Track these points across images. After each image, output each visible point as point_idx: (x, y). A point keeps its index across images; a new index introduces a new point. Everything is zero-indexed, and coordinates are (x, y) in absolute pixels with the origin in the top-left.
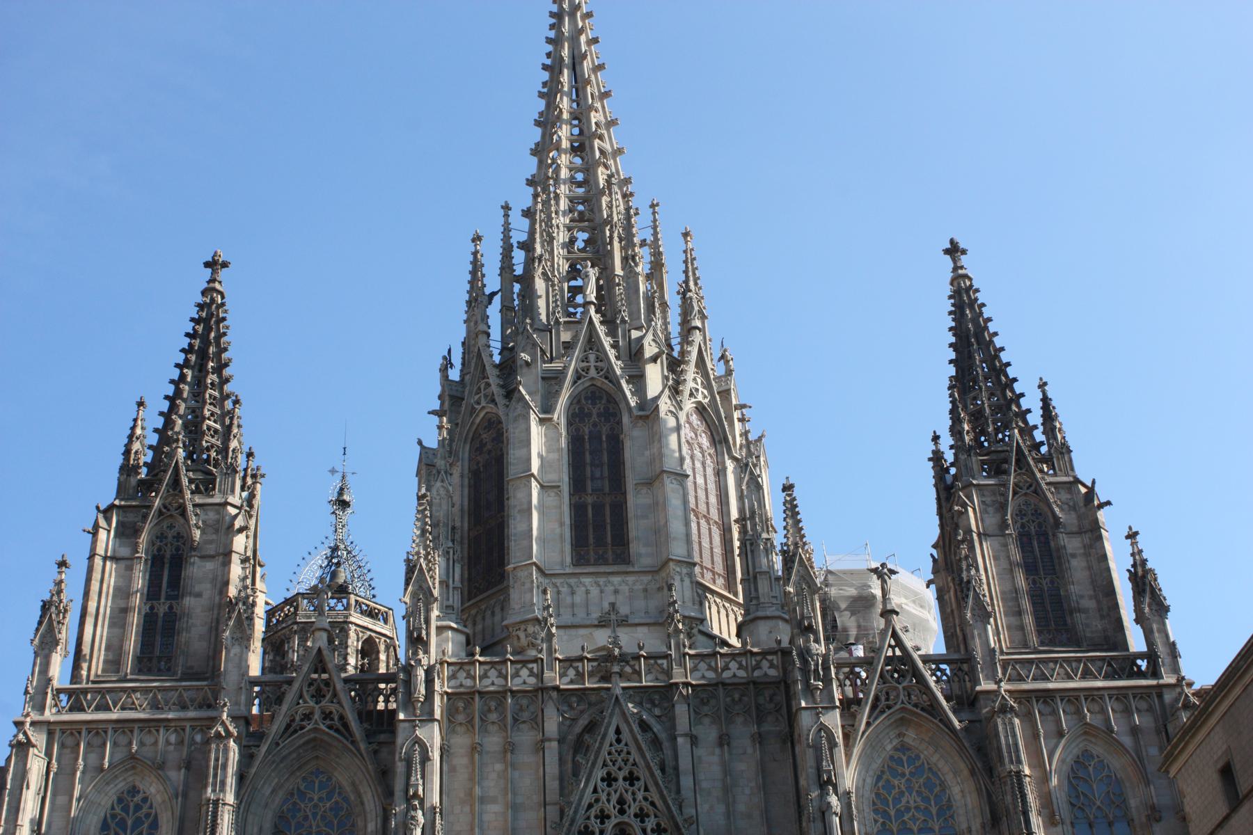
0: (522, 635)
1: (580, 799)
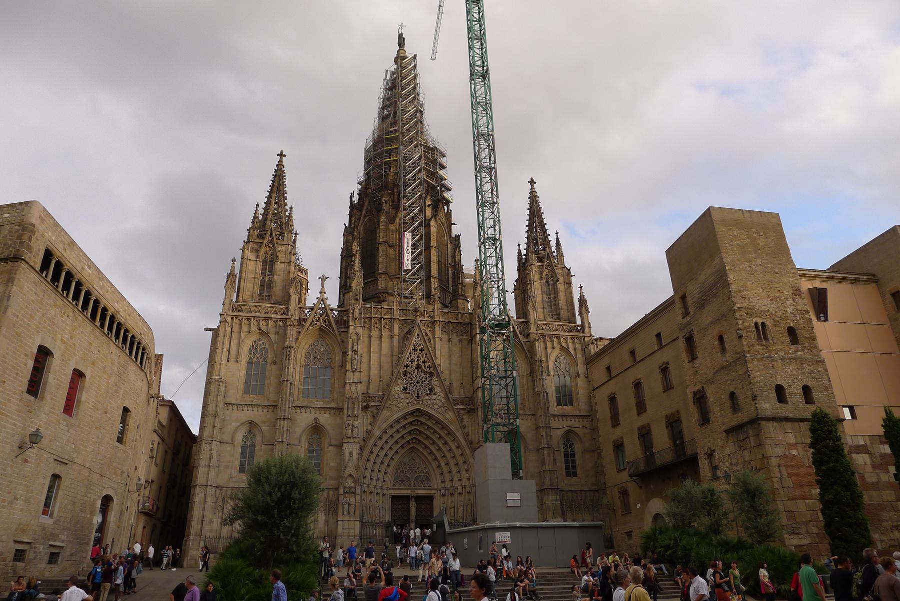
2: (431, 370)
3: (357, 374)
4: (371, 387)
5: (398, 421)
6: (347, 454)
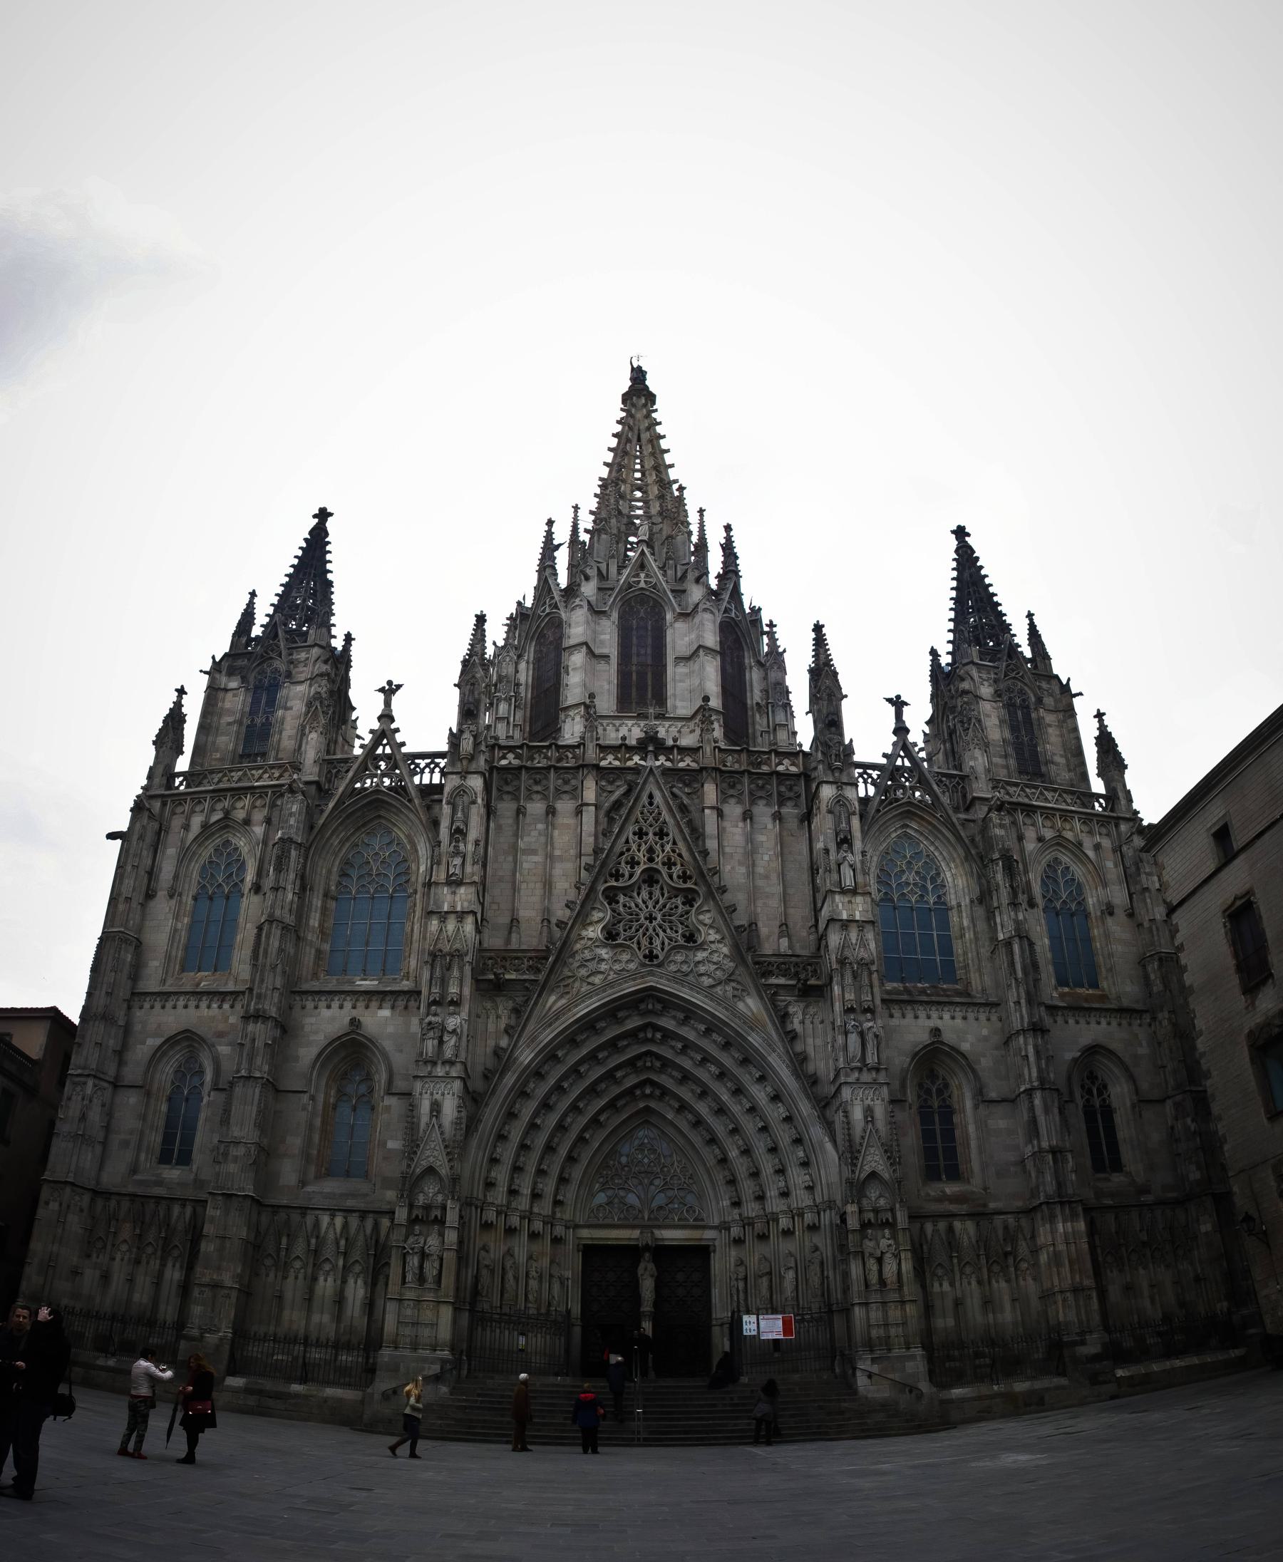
2: (689, 885)
4: (514, 937)
5: (589, 1024)
6: (425, 1106)
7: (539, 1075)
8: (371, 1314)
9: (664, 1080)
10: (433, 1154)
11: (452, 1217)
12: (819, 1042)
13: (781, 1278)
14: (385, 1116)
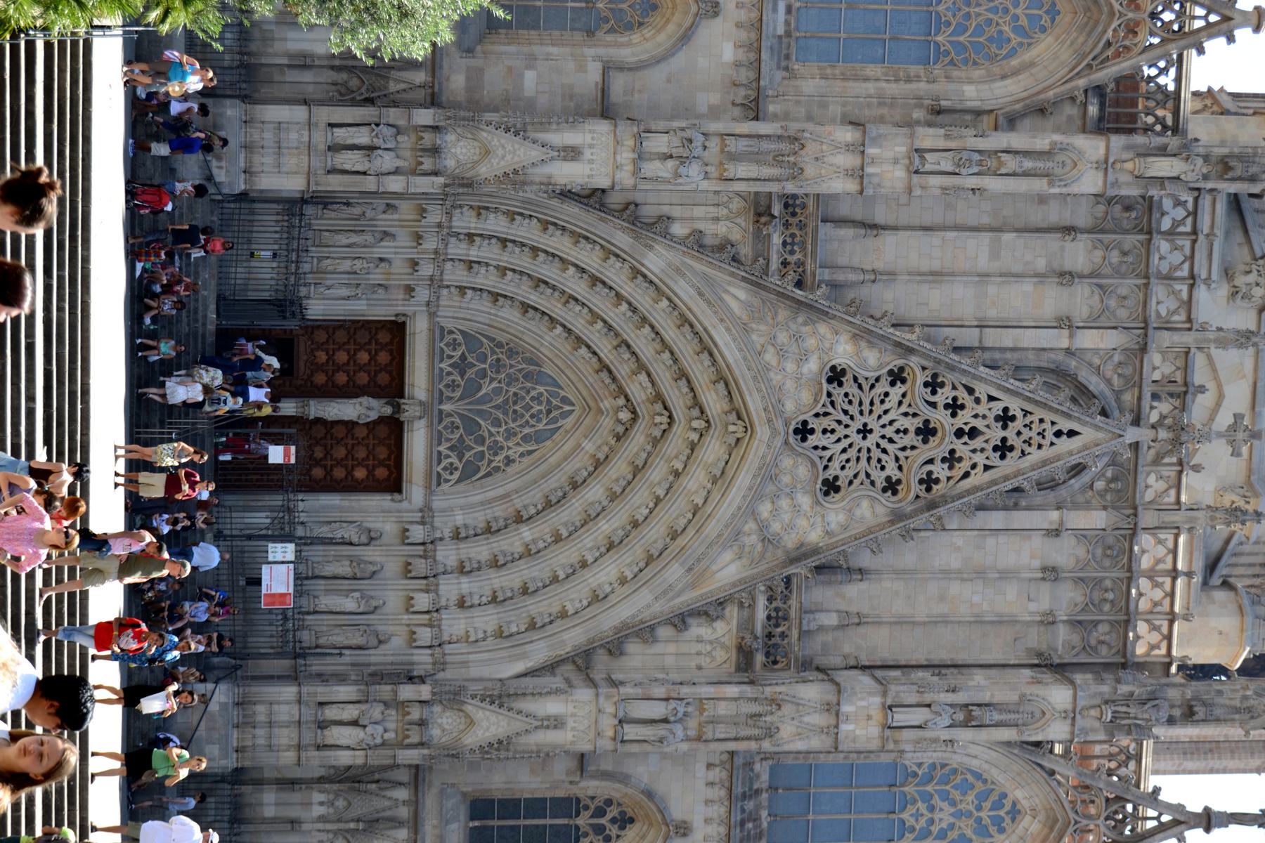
0: (1251, 278)
1: (981, 379)
3: (900, 173)
7: (636, 273)
8: (290, 66)
9: (638, 439)
10: (508, 153)
11: (424, 184)
12: (670, 661)
13: (347, 593)
14: (571, 65)
